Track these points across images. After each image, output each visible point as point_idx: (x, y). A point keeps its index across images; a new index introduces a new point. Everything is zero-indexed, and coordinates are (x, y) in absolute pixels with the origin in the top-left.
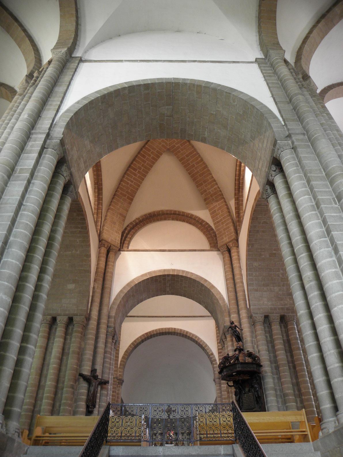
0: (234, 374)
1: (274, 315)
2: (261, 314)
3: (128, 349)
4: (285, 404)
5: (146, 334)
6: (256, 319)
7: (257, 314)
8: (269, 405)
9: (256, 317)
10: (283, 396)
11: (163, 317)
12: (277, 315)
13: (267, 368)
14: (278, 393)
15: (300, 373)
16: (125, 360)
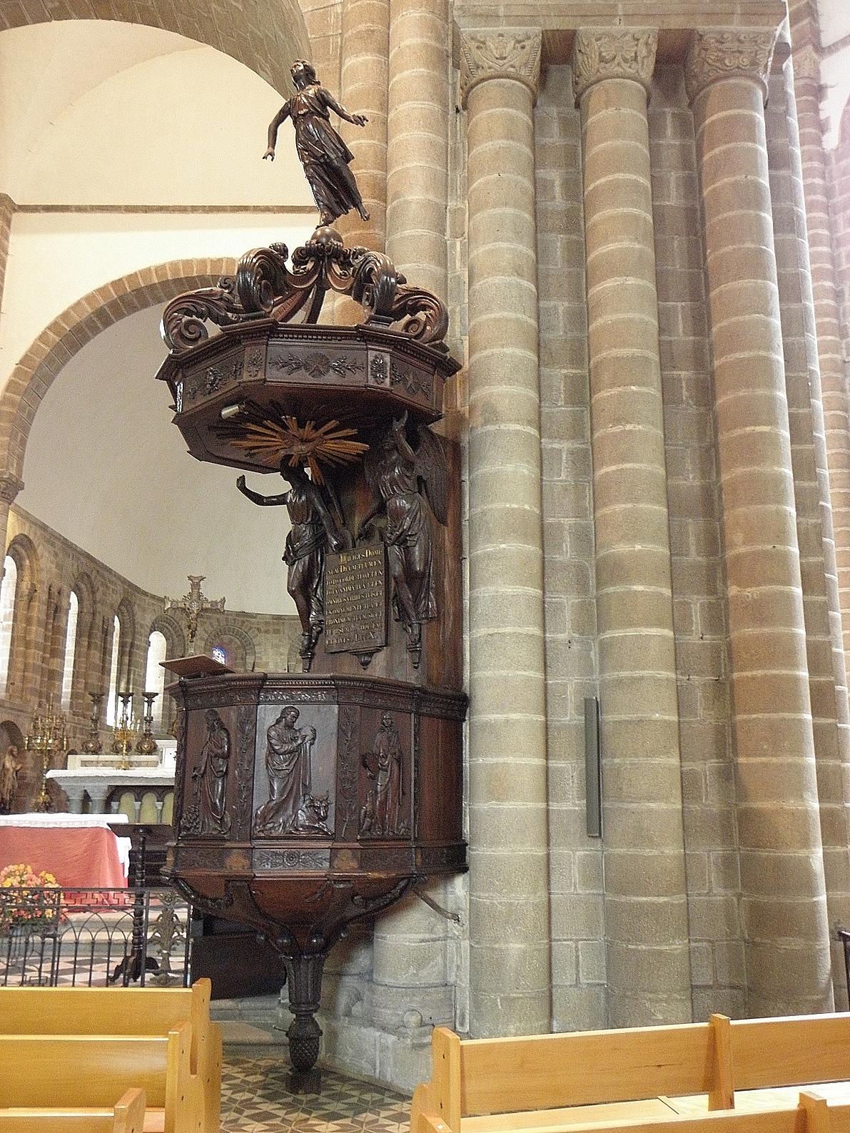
0: (226, 412)
1: (618, 27)
2: (512, 19)
3: (34, 349)
4: (600, 630)
5: (117, 284)
6: (477, 55)
7: (490, 17)
8: (482, 631)
9: (482, 45)
10: (592, 573)
11: (194, 209)
12: (634, 29)
13: (504, 389)
14: (566, 553)
15: (739, 432)
16: (18, 398)
